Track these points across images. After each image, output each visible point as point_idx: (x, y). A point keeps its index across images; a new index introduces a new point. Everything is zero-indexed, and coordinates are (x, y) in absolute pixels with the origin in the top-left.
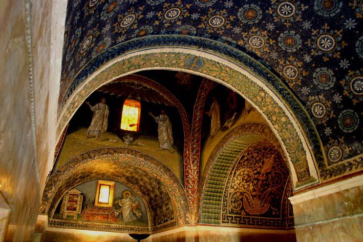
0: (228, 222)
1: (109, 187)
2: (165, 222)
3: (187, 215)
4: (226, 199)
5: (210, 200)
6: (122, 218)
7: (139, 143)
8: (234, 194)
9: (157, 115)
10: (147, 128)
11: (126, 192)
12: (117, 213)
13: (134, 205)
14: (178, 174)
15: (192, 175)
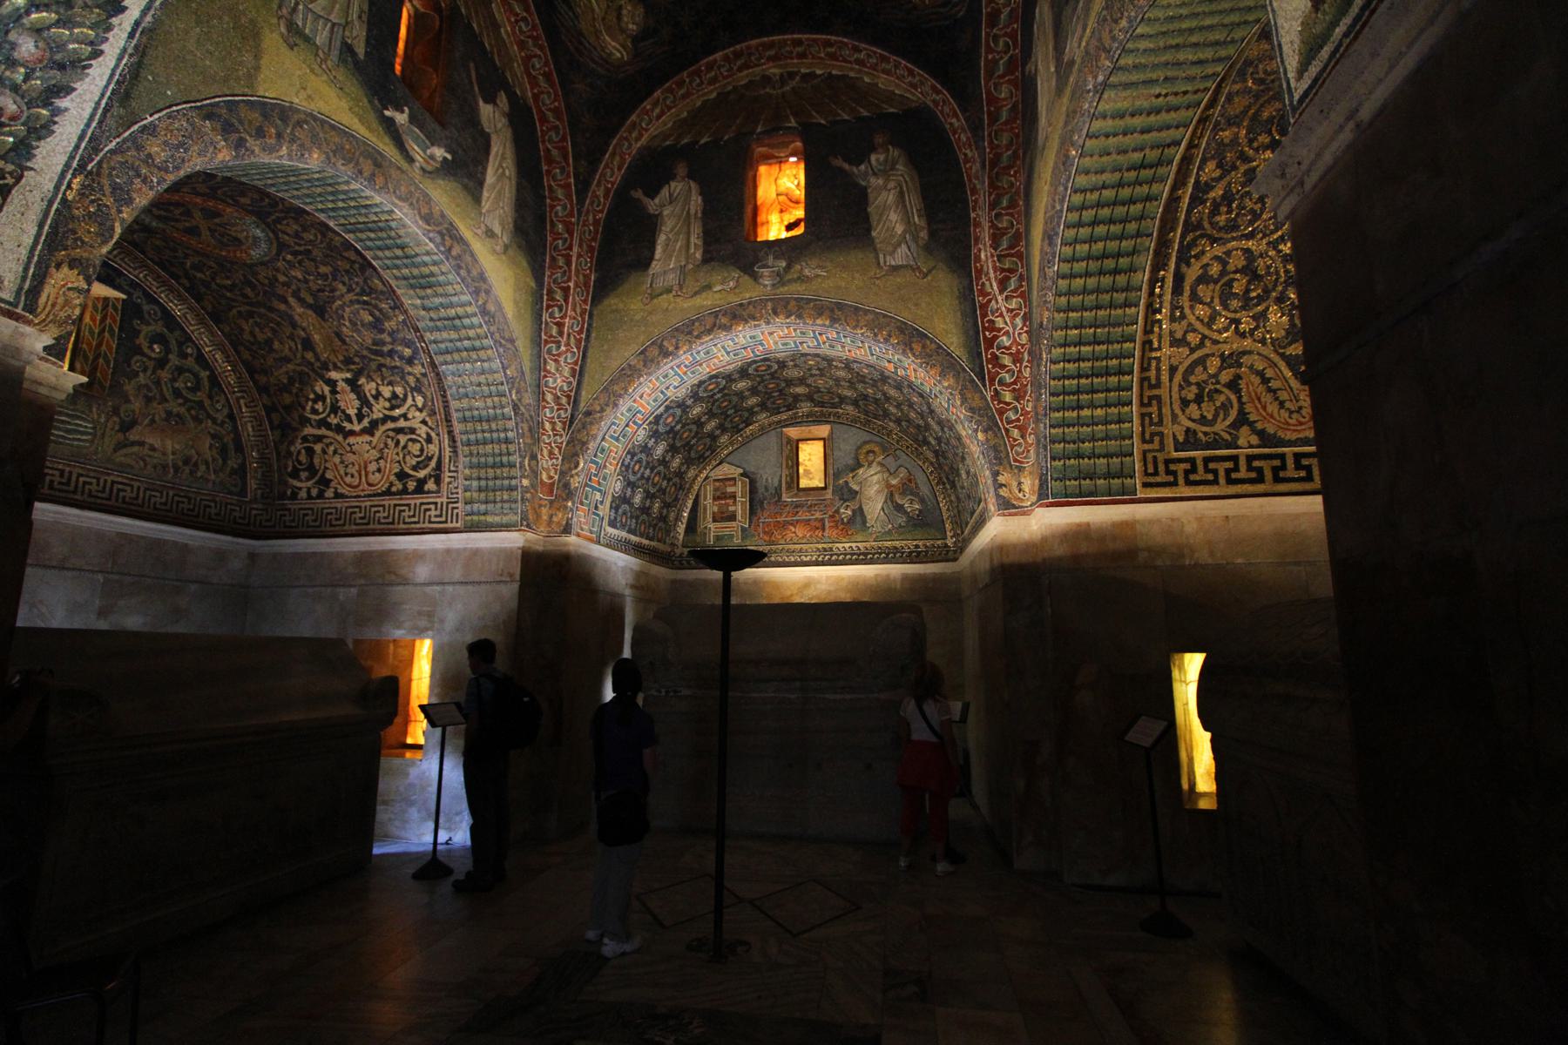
0: (1175, 484)
1: (821, 443)
2: (972, 513)
3: (1001, 479)
4: (1156, 392)
5: (1080, 407)
6: (864, 522)
7: (807, 272)
8: (1190, 370)
9: (860, 157)
10: (836, 216)
11: (868, 447)
12: (846, 513)
13: (894, 482)
14: (954, 342)
15: (1007, 333)
